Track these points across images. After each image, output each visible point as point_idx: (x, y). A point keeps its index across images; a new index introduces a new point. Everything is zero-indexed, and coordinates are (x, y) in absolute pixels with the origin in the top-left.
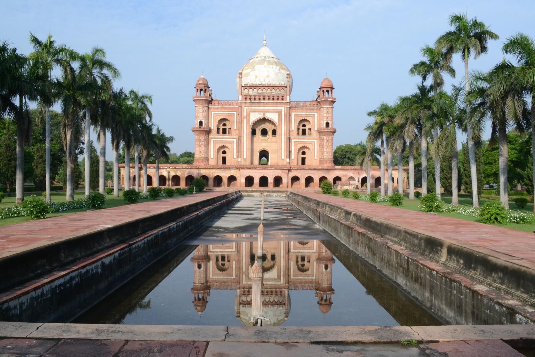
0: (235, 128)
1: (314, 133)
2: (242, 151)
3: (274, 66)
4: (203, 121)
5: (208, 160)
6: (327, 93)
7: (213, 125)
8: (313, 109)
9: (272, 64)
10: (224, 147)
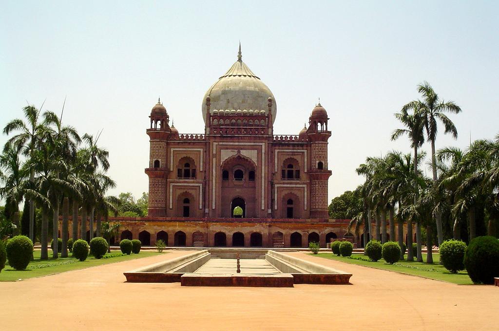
1: (303, 176)
2: (210, 199)
4: (160, 160)
5: (166, 211)
6: (319, 124)
8: (302, 145)
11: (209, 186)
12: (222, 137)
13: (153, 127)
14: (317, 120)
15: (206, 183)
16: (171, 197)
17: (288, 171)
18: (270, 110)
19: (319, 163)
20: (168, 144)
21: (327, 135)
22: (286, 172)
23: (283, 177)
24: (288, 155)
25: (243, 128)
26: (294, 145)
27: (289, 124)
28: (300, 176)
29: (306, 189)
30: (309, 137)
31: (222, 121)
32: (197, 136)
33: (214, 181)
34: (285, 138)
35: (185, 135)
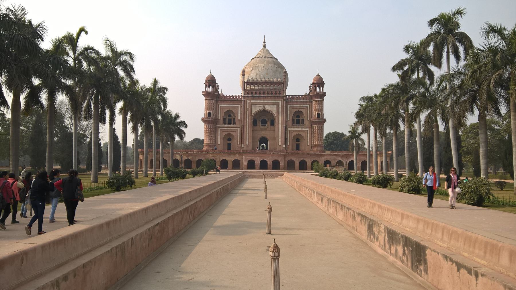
1: (307, 123)
3: (273, 65)
4: (211, 112)
7: (220, 117)
9: (271, 63)
15: (243, 128)
16: (219, 137)
19: (318, 114)
20: (216, 101)
21: (322, 95)
22: (295, 120)
23: (293, 123)
27: (297, 87)
31: (252, 87)
33: (247, 126)
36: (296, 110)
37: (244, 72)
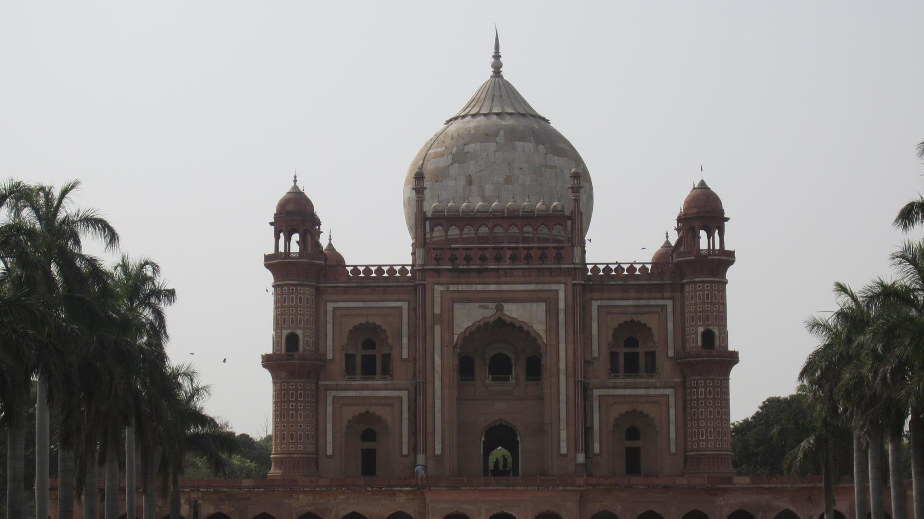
0: (405, 355)
1: (664, 366)
2: (429, 430)
3: (530, 146)
4: (299, 332)
6: (703, 234)
7: (331, 349)
8: (660, 288)
9: (523, 139)
10: (367, 417)
11: (425, 395)
12: (458, 273)
13: (281, 249)
14: (696, 224)
15: (419, 392)
16: (329, 426)
17: (626, 354)
18: (577, 201)
20: (318, 290)
23: (614, 369)
24: (625, 313)
25: (509, 248)
26: (639, 289)
27: (625, 232)
28: (657, 366)
29: (672, 401)
30: (678, 265)
31: (454, 232)
32: (392, 270)
33: (438, 384)
34: (616, 269)
35: (361, 269)
36: (623, 319)
37: (419, 177)
